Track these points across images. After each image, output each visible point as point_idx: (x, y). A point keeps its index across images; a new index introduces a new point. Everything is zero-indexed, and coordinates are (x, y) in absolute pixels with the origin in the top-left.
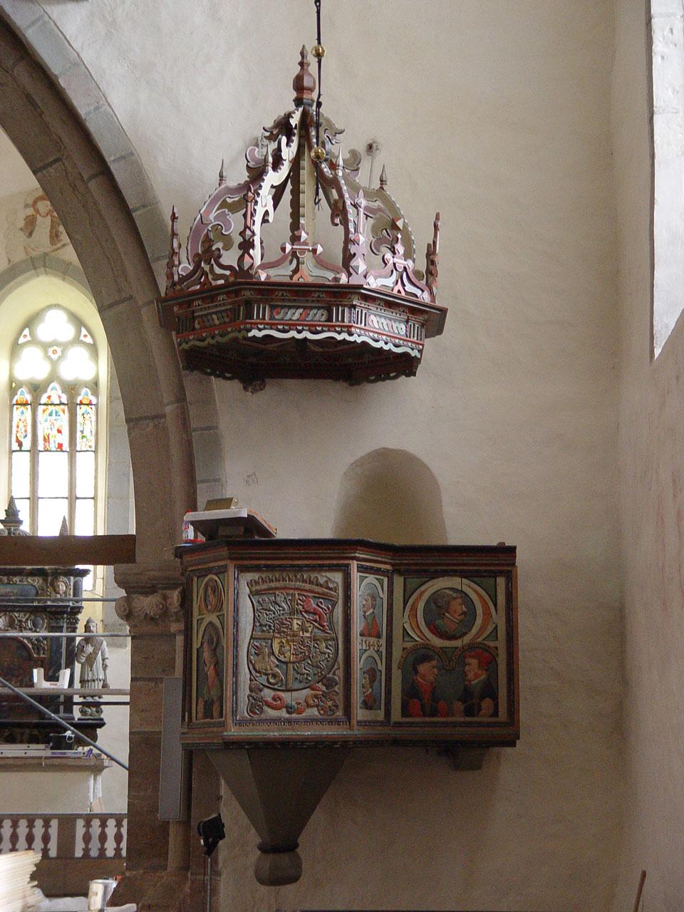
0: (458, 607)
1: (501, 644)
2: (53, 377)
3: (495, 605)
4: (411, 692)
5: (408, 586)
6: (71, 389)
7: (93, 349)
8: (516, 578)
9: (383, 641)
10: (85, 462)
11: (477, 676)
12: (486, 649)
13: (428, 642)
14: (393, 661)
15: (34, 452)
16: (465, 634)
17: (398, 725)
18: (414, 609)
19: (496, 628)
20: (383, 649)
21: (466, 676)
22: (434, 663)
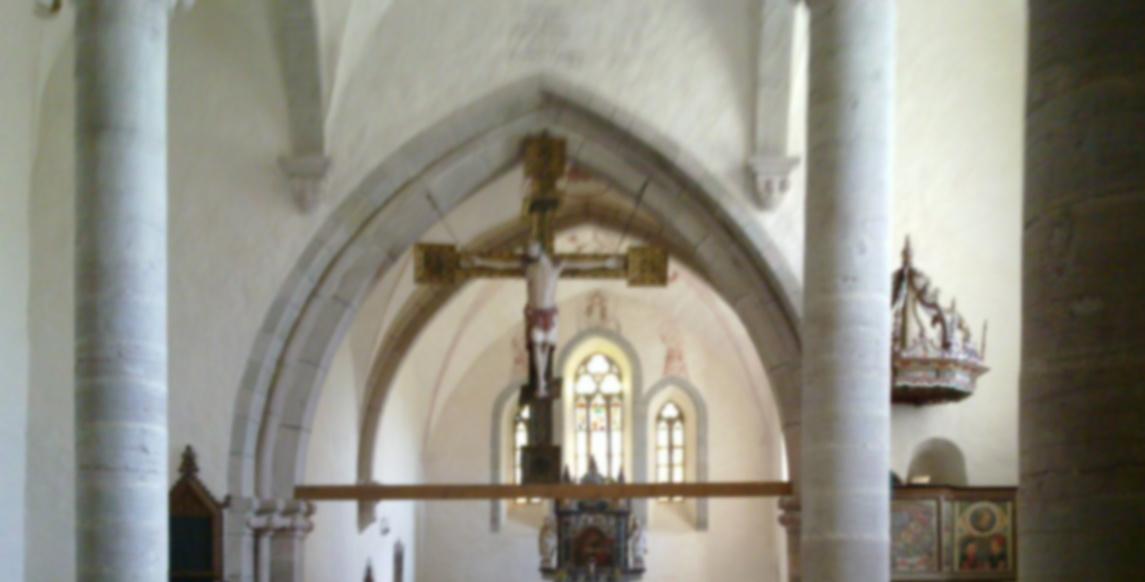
2: (598, 391)
4: (964, 558)
6: (608, 398)
7: (620, 376)
10: (616, 436)
15: (589, 432)
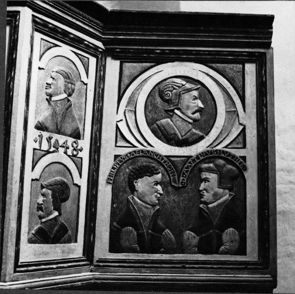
0: (192, 102)
1: (250, 153)
3: (243, 99)
5: (126, 72)
8: (272, 63)
9: (85, 143)
11: (216, 196)
12: (230, 159)
13: (149, 148)
14: (100, 173)
16: (201, 138)
17: (104, 264)
18: (132, 101)
19: (244, 130)
20: (85, 155)
21: (202, 196)
22: (159, 176)
